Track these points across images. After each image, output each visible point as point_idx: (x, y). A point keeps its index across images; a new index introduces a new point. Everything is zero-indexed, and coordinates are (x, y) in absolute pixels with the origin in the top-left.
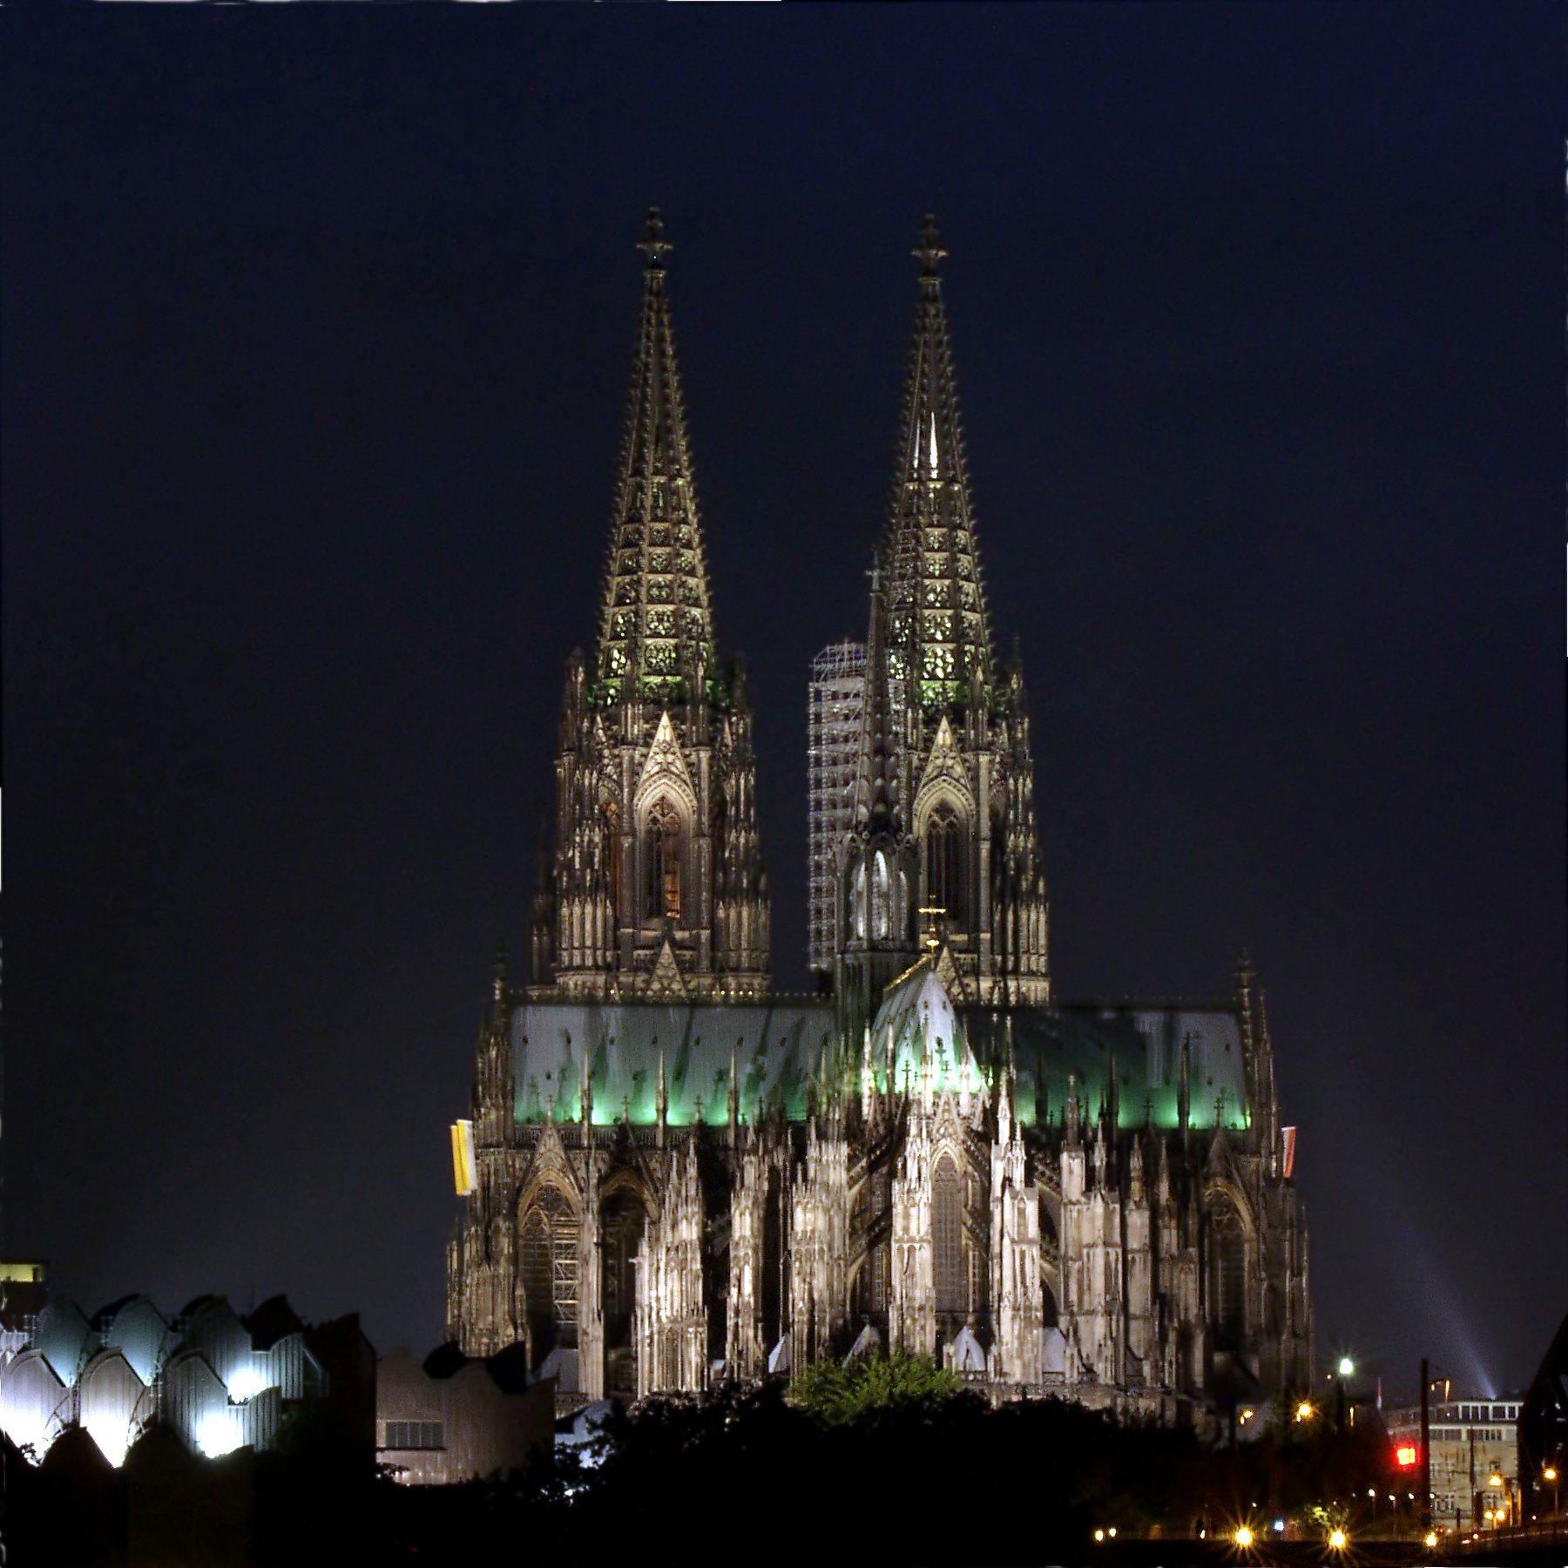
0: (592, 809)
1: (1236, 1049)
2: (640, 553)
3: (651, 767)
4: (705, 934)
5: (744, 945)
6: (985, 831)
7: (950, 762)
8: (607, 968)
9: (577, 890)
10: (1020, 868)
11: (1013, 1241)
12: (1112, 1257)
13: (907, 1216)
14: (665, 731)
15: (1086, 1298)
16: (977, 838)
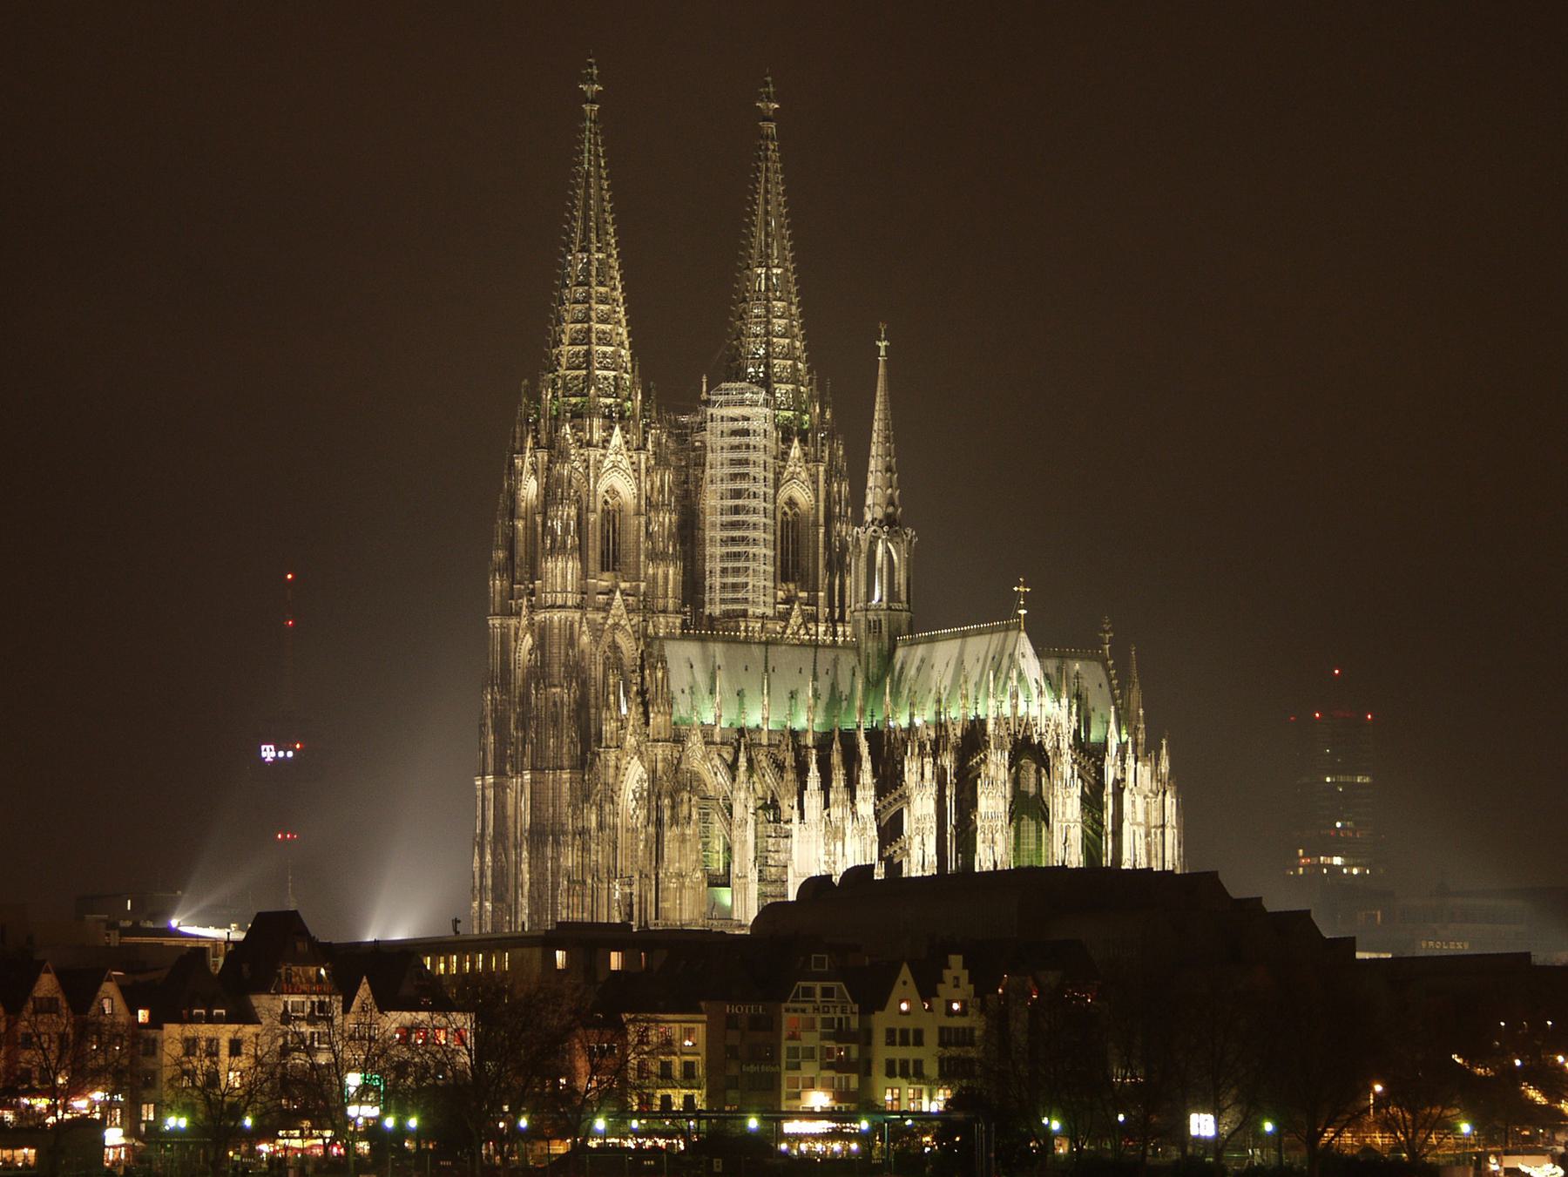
1: (1106, 688)
2: (590, 308)
3: (607, 463)
5: (670, 593)
6: (822, 520)
8: (579, 607)
9: (558, 549)
14: (617, 438)
16: (816, 524)
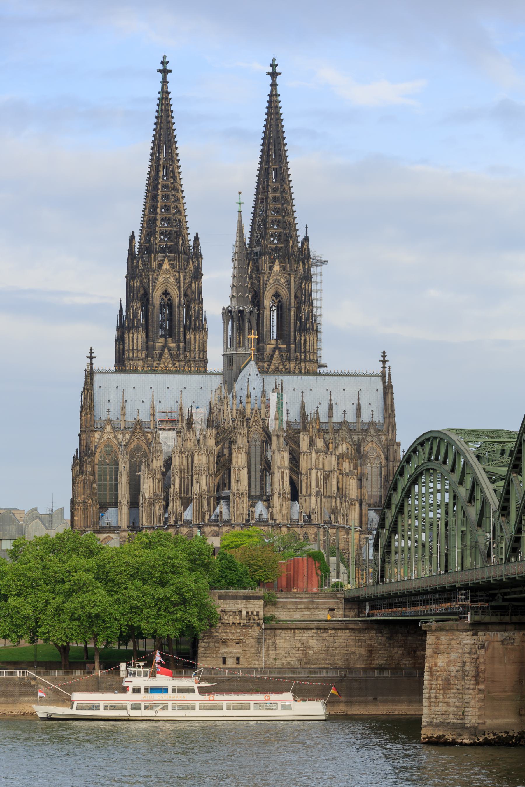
0: (138, 296)
3: (161, 279)
4: (182, 345)
7: (279, 277)
10: (307, 319)
11: (279, 468)
12: (319, 473)
13: (237, 457)
15: (309, 489)
